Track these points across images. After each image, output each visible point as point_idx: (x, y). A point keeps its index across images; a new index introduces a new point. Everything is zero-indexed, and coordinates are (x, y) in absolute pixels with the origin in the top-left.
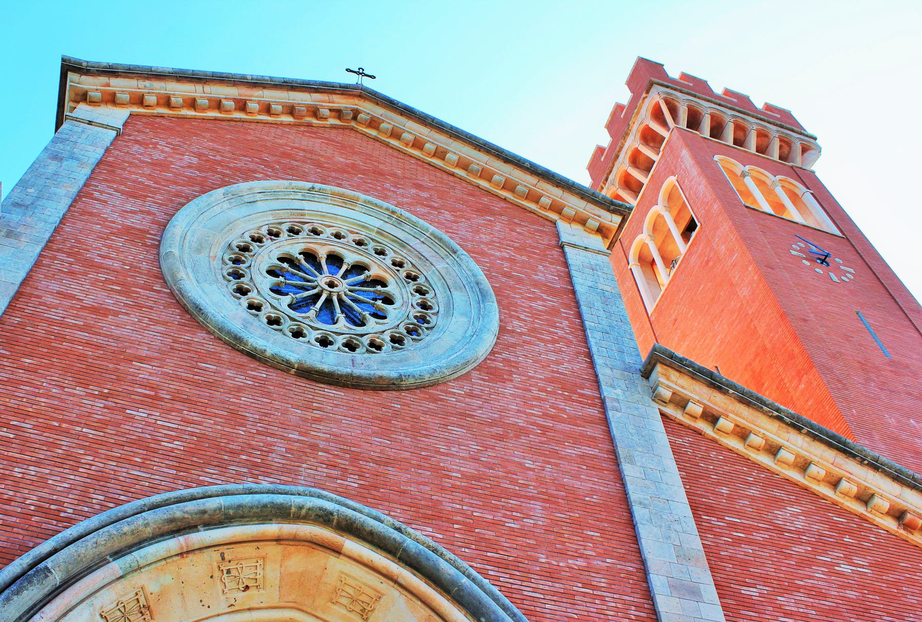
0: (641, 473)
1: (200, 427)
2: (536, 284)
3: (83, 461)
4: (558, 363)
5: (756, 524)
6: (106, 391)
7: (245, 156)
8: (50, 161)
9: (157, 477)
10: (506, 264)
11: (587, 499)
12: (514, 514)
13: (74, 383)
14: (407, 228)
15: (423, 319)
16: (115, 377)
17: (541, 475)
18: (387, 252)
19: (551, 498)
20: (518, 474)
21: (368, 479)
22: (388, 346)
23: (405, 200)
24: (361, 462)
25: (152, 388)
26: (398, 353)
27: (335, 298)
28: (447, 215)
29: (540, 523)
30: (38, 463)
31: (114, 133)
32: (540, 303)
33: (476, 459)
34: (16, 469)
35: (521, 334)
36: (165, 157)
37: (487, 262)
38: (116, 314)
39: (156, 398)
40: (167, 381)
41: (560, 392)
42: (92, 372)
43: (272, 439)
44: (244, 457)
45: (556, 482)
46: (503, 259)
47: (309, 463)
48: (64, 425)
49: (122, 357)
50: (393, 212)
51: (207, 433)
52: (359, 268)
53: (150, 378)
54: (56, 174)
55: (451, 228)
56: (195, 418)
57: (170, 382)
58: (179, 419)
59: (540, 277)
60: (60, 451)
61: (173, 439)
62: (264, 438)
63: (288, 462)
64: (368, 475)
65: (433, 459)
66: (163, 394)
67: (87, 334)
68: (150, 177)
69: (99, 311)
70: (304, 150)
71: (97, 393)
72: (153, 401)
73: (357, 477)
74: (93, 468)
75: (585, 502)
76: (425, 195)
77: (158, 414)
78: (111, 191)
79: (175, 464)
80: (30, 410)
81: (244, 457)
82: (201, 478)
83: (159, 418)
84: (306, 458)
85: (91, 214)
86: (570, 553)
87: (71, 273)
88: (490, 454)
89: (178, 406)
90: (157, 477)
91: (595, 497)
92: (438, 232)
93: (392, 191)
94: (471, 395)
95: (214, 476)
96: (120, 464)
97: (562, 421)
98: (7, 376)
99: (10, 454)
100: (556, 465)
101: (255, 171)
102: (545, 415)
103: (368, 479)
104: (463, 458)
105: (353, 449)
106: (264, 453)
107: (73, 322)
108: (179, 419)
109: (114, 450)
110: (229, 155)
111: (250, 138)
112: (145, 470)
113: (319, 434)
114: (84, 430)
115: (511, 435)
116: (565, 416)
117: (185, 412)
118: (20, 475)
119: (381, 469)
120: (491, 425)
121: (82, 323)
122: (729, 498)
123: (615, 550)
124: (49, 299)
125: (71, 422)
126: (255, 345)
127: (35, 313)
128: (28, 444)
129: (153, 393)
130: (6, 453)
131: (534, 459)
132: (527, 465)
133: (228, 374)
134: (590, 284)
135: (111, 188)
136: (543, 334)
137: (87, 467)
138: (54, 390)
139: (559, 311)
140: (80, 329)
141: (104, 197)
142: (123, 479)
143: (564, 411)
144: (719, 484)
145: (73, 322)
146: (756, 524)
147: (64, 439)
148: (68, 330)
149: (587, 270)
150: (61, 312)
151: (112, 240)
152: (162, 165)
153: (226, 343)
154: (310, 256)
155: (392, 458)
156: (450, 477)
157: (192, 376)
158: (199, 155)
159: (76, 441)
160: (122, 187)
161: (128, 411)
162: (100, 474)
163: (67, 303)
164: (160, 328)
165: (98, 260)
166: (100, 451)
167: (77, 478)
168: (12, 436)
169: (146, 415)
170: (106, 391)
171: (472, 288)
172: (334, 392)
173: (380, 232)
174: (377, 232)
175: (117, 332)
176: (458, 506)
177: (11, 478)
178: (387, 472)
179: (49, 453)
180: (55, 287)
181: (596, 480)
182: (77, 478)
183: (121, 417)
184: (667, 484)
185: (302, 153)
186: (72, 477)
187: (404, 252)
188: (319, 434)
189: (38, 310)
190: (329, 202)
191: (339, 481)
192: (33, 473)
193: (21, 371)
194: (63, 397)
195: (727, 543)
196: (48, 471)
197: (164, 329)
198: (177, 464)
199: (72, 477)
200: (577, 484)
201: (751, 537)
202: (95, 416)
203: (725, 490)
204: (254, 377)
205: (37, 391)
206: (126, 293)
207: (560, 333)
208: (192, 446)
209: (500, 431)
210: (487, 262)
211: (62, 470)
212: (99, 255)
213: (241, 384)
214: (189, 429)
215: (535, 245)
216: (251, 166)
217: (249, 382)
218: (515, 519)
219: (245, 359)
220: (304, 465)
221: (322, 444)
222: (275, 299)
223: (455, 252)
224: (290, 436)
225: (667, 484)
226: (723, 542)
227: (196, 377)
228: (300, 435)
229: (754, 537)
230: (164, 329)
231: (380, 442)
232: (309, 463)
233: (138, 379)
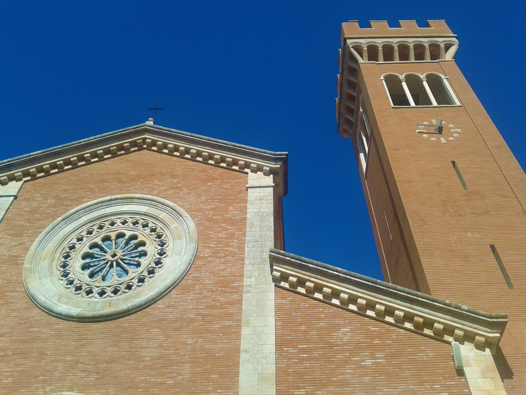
0: (251, 331)
1: (24, 366)
5: (317, 346)
10: (212, 213)
11: (217, 355)
12: (173, 375)
17: (194, 346)
19: (196, 360)
20: (182, 349)
24: (99, 364)
29: (186, 377)
32: (224, 232)
33: (161, 346)
36: (38, 204)
41: (220, 289)
44: (41, 378)
47: (73, 372)
58: (13, 364)
61: (8, 377)
64: (101, 371)
66: (9, 353)
75: (216, 357)
76: (175, 181)
77: (4, 365)
81: (41, 378)
86: (198, 391)
91: (222, 352)
94: (167, 307)
100: (205, 338)
101: (83, 198)
104: (154, 348)
105: (97, 358)
106: (52, 373)
111: (86, 175)
122: (306, 331)
123: (225, 383)
131: (193, 338)
133: (44, 331)
135: (6, 234)
136: (220, 253)
139: (234, 234)
143: (218, 301)
144: (301, 324)
146: (317, 346)
155: (116, 357)
156: (143, 361)
157: (25, 338)
160: (12, 232)
172: (95, 326)
176: (144, 378)
184: (265, 334)
195: (295, 363)
197: (17, 314)
200: (214, 346)
201: (312, 355)
203: (303, 328)
204: (56, 329)
218: (172, 378)
220: (70, 374)
225: (265, 334)
226: (292, 363)
227: (27, 338)
228: (72, 357)
229: (313, 355)
230: (17, 314)
231: (112, 350)
232: (73, 372)
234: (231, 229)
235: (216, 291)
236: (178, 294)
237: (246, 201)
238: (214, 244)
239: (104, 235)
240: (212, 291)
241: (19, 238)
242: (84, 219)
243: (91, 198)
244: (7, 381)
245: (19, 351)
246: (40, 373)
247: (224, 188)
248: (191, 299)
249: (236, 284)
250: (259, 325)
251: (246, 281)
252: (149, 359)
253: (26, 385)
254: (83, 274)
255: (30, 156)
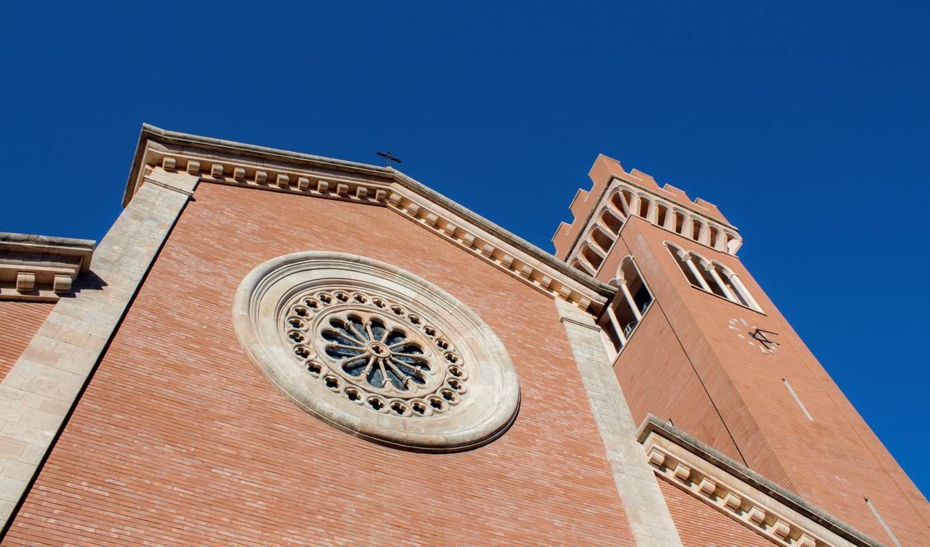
0: (647, 531)
2: (545, 355)
3: (175, 521)
4: (570, 428)
6: (193, 449)
7: (299, 226)
8: (132, 220)
9: (244, 538)
13: (162, 441)
14: (438, 300)
15: (454, 385)
16: (199, 435)
18: (420, 321)
20: (550, 532)
21: (428, 539)
22: (429, 409)
23: (434, 274)
24: (420, 522)
25: (234, 447)
26: (438, 417)
27: (381, 363)
28: (469, 290)
30: (133, 523)
31: (186, 197)
32: (549, 372)
33: (515, 519)
34: (113, 530)
35: (538, 401)
36: (231, 223)
37: (504, 334)
38: (197, 372)
39: (238, 457)
40: (247, 441)
42: (179, 430)
43: (343, 500)
44: (320, 517)
45: (580, 539)
46: (516, 331)
48: (156, 484)
49: (205, 415)
50: (425, 286)
51: (286, 493)
52: (397, 334)
53: (232, 437)
54: (137, 233)
55: (472, 302)
56: (274, 478)
57: (250, 442)
59: (547, 348)
60: (153, 510)
62: (336, 498)
63: (359, 523)
64: (427, 535)
65: (480, 519)
66: (245, 454)
67: (172, 392)
68: (219, 240)
69: (181, 368)
70: (348, 224)
71: (184, 451)
72: (235, 461)
73: (418, 537)
74: (185, 528)
76: (448, 270)
77: (241, 474)
78: (186, 252)
79: (260, 524)
80: (123, 467)
81: (320, 517)
82: (284, 539)
83: (242, 478)
84: (374, 519)
85: (170, 274)
87: (155, 330)
88: (525, 514)
89: (258, 465)
90: (244, 538)
92: (464, 306)
93: (423, 266)
94: (503, 458)
95: (295, 537)
96: (210, 525)
97: (579, 482)
98: (100, 431)
99: (106, 513)
100: (580, 524)
101: (307, 241)
102: (566, 478)
103: (428, 539)
105: (412, 510)
107: (160, 379)
108: (260, 479)
109: (204, 509)
110: (285, 224)
111: (302, 209)
112: (230, 529)
113: (383, 495)
114: (175, 489)
115: (540, 496)
116: (581, 478)
117: (265, 472)
118: (116, 536)
119: (438, 529)
120: (523, 486)
121: (167, 381)
124: (137, 355)
125: (162, 480)
126: (322, 408)
127: (124, 368)
128: (122, 503)
129: (234, 453)
130: (102, 512)
132: (556, 524)
133: (300, 435)
134: (588, 356)
135: (186, 249)
136: (554, 401)
137: (180, 527)
138: (145, 448)
139: (566, 381)
140: (167, 386)
141: (180, 258)
142: (213, 539)
143: (578, 472)
145: (160, 379)
147: (157, 497)
148: (155, 387)
149: (584, 344)
150: (148, 368)
151: (189, 299)
152: (228, 230)
153: (296, 404)
154: (356, 320)
155: (445, 518)
156: (494, 536)
157: (268, 436)
158: (260, 223)
159: (168, 500)
160: (196, 249)
161: (214, 470)
162: (192, 534)
163: (153, 359)
164: (236, 388)
165: (178, 318)
166: (191, 511)
167: (171, 539)
168: (107, 494)
169: (230, 475)
170: (193, 449)
171: (495, 357)
173: (415, 302)
174: (412, 303)
175: (200, 390)
177: (108, 539)
178: (442, 532)
179: (143, 513)
180: (140, 342)
181: (612, 537)
182: (171, 539)
183: (207, 476)
185: (345, 227)
186: (166, 538)
187: (435, 322)
188: (383, 495)
189: (126, 365)
190: (372, 273)
191: (404, 541)
192: (129, 534)
193: (114, 427)
194: (154, 454)
196: (143, 532)
197: (240, 389)
198: (262, 525)
199: (166, 538)
202: (185, 475)
205: (129, 447)
206: (205, 352)
207: (569, 400)
208: (274, 506)
209: (531, 492)
210: (504, 334)
211: (156, 530)
212: (179, 314)
213: (312, 445)
214: (270, 489)
215: (540, 319)
216: (305, 236)
217: (319, 444)
219: (314, 420)
221: (386, 505)
222: (332, 362)
223: (479, 325)
224: (359, 496)
230: (240, 389)
231: (435, 503)
233: (220, 438)
234: (560, 371)
235: (569, 456)
236: (512, 444)
237: (565, 337)
238: (541, 385)
239: (351, 311)
240: (560, 453)
241: (212, 265)
242: (316, 275)
243: (320, 246)
244: (255, 505)
245: (264, 457)
246: (316, 508)
247: (527, 308)
248: (537, 458)
249: (595, 455)
250: (655, 525)
251: (611, 455)
252: (503, 535)
253: (296, 524)
254: (334, 362)
255: (220, 144)
